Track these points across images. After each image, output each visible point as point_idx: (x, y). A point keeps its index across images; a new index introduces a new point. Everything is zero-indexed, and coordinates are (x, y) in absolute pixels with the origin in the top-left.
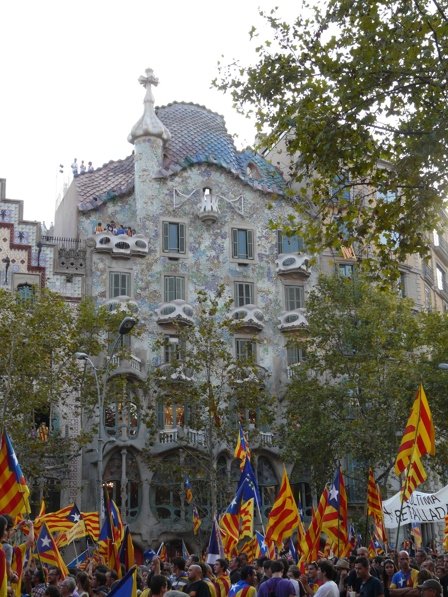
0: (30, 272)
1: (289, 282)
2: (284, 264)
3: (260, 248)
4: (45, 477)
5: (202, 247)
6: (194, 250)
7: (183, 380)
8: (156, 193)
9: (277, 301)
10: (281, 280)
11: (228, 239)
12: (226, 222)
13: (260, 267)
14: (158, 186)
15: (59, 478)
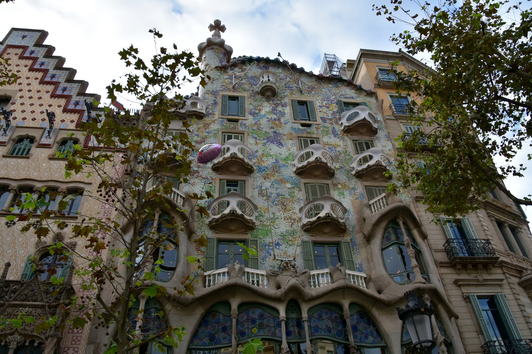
0: (78, 129)
1: (355, 137)
2: (348, 120)
3: (322, 113)
4: (20, 334)
5: (263, 112)
6: (253, 114)
7: (237, 215)
8: (217, 77)
9: (346, 152)
10: (347, 136)
11: (288, 107)
12: (285, 96)
13: (324, 126)
14: (219, 74)
15: (43, 336)
